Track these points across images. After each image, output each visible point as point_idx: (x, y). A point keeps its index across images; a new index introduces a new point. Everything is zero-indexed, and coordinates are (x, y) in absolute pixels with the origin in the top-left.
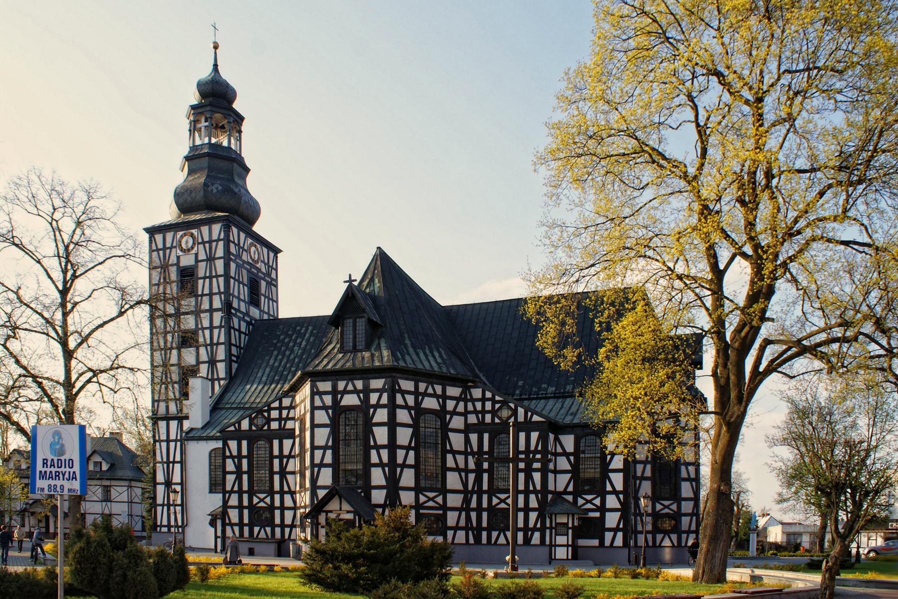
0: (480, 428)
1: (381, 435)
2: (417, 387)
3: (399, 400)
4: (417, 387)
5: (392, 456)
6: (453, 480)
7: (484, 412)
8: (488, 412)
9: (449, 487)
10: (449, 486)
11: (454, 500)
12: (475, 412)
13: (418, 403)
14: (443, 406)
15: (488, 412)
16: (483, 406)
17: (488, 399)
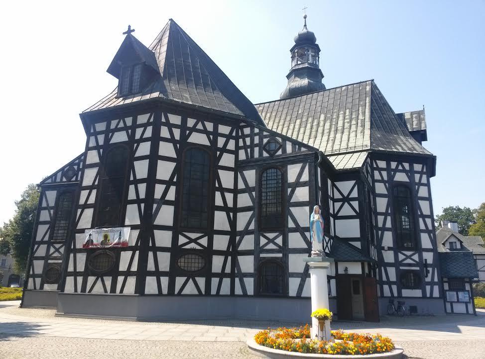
0: (248, 164)
1: (141, 169)
2: (184, 121)
3: (164, 132)
4: (184, 121)
5: (150, 191)
6: (221, 220)
7: (252, 146)
8: (256, 145)
9: (216, 227)
10: (216, 227)
11: (221, 243)
12: (245, 147)
13: (184, 137)
14: (214, 142)
15: (256, 145)
16: (252, 141)
17: (256, 134)
